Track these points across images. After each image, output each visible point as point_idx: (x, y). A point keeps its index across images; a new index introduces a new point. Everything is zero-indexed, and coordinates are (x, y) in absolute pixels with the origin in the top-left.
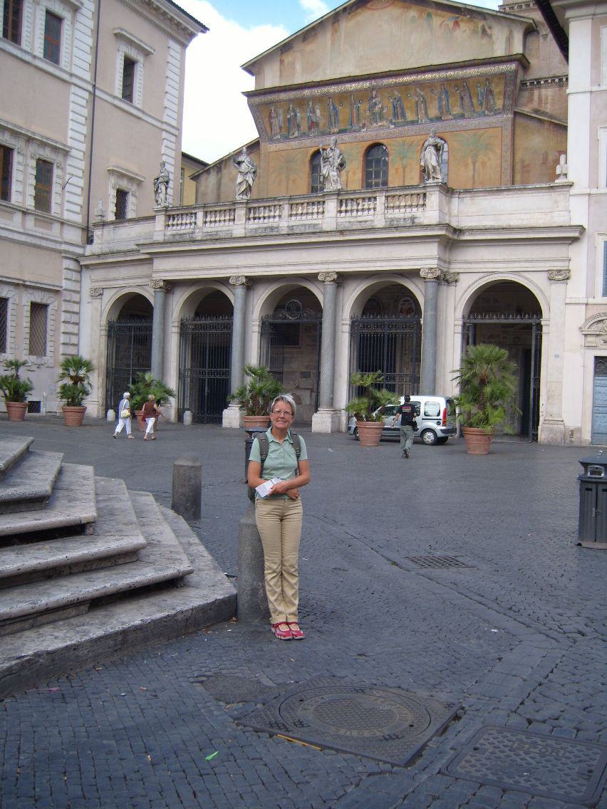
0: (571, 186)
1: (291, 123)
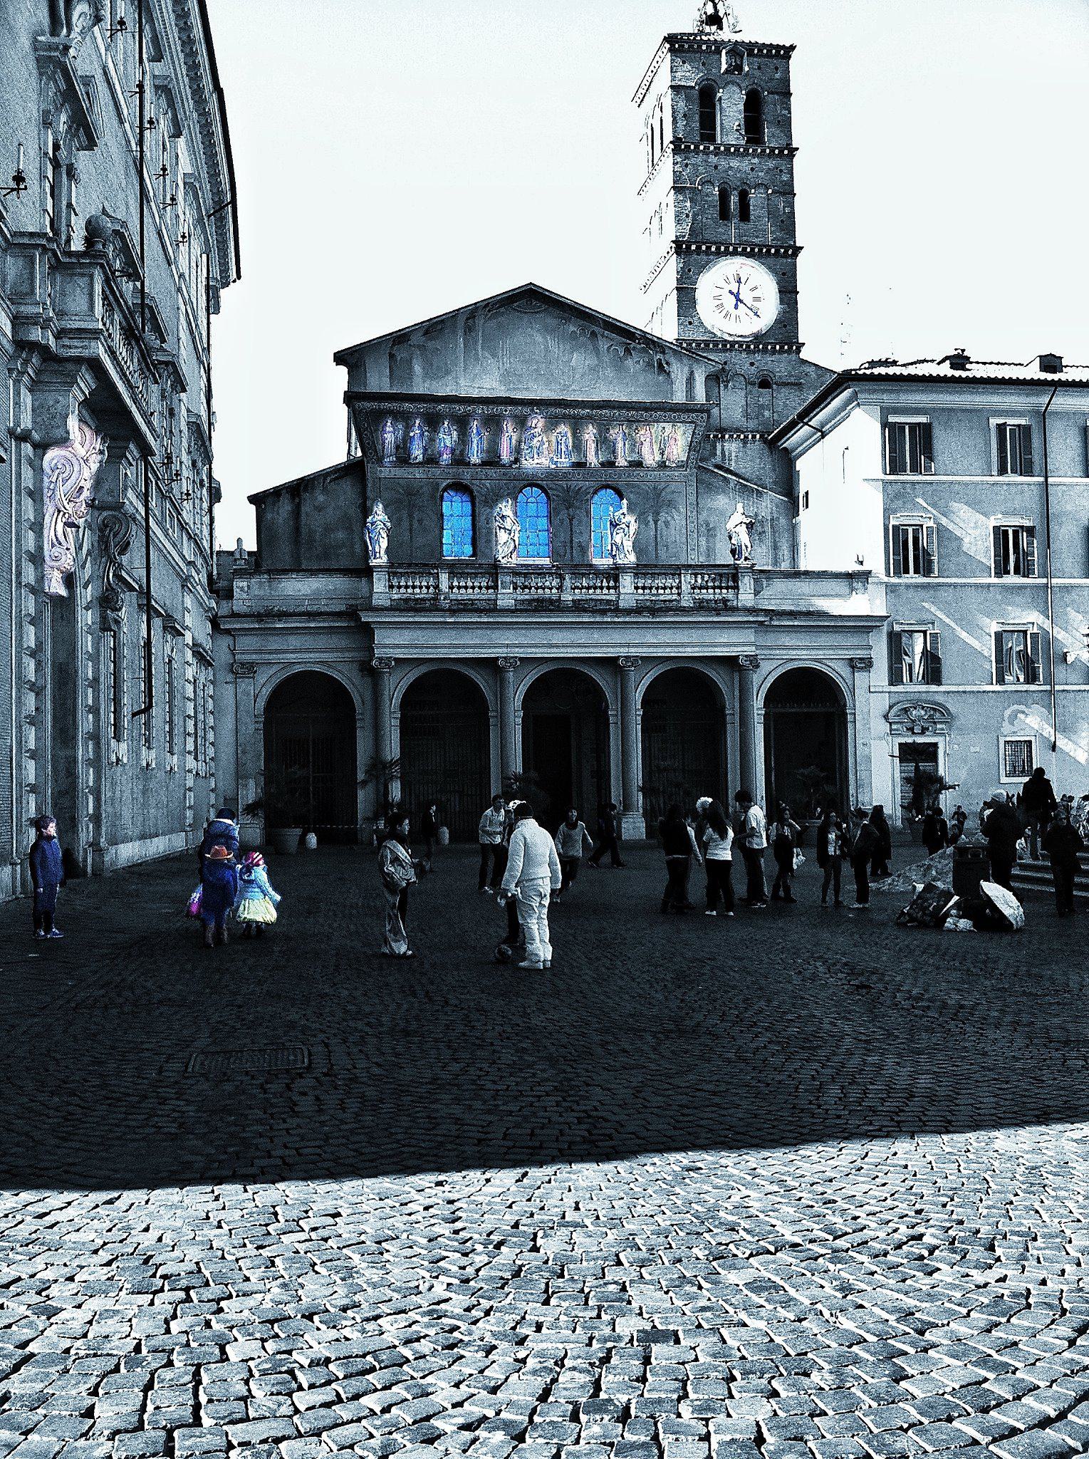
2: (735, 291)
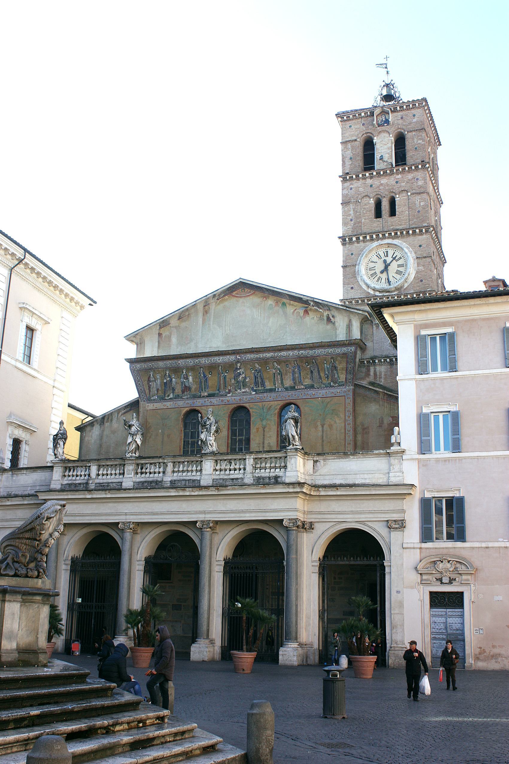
0: (404, 452)
1: (167, 386)
2: (388, 262)
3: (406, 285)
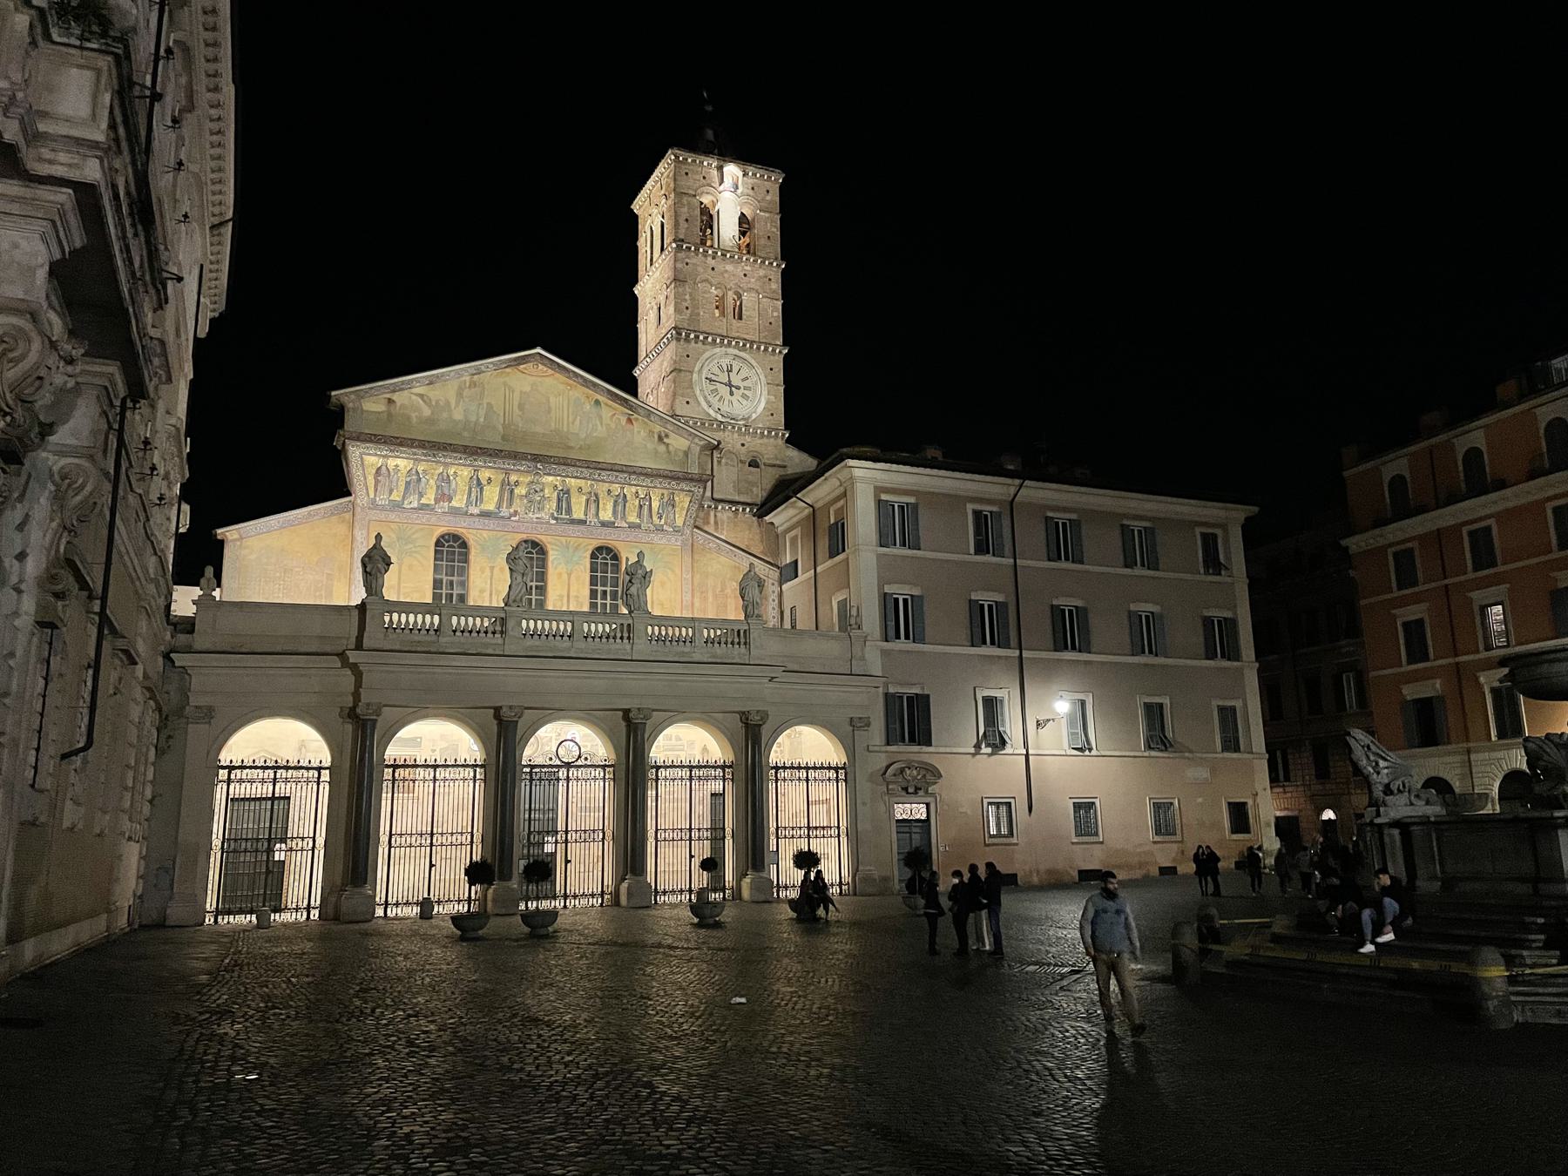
3: (754, 416)
